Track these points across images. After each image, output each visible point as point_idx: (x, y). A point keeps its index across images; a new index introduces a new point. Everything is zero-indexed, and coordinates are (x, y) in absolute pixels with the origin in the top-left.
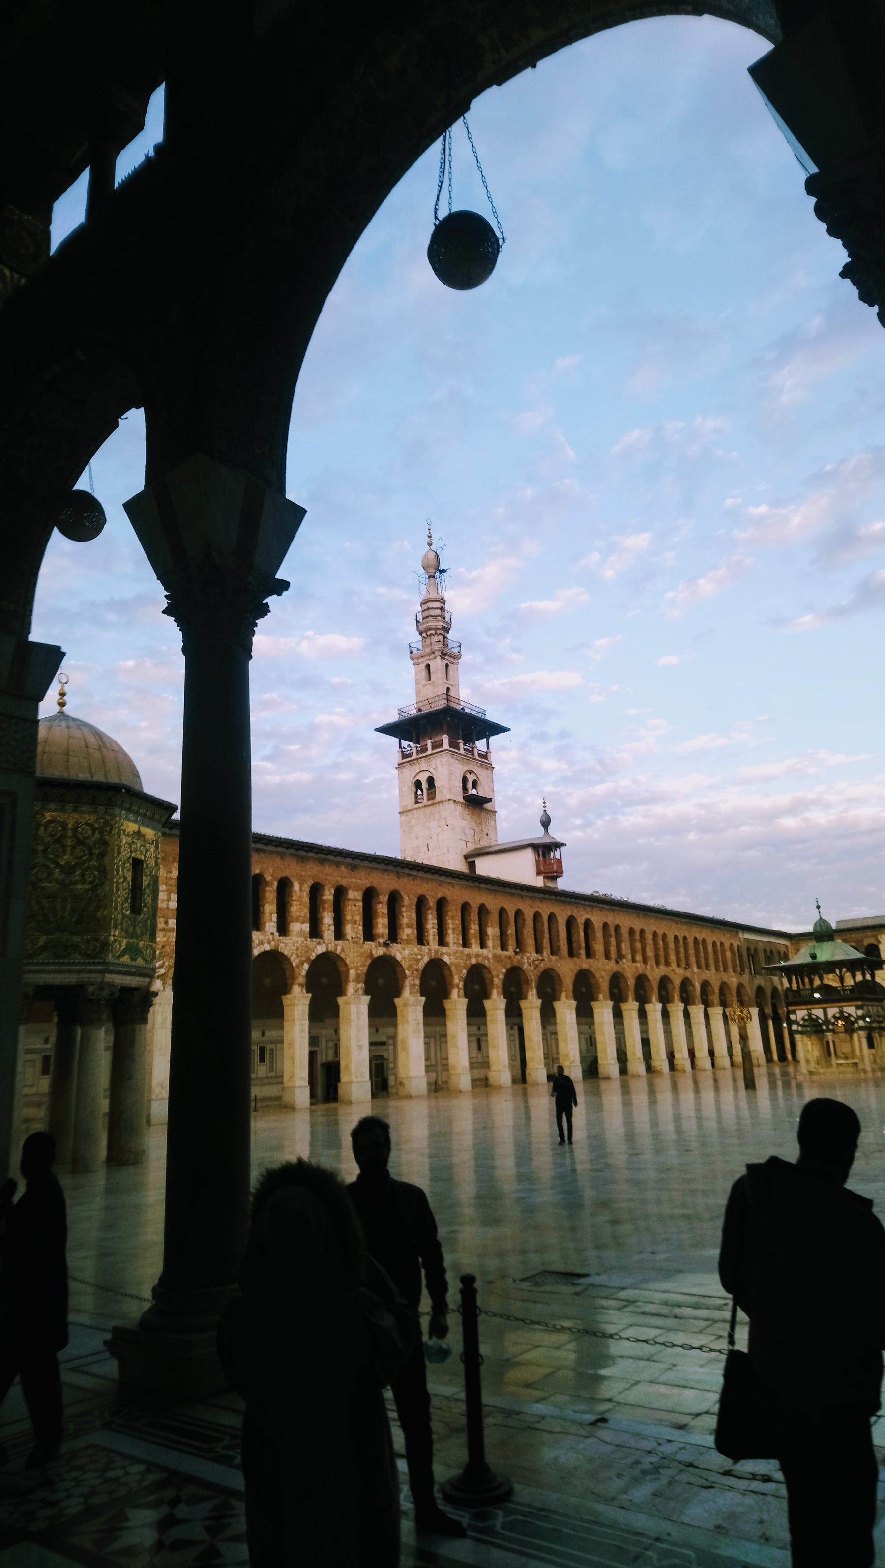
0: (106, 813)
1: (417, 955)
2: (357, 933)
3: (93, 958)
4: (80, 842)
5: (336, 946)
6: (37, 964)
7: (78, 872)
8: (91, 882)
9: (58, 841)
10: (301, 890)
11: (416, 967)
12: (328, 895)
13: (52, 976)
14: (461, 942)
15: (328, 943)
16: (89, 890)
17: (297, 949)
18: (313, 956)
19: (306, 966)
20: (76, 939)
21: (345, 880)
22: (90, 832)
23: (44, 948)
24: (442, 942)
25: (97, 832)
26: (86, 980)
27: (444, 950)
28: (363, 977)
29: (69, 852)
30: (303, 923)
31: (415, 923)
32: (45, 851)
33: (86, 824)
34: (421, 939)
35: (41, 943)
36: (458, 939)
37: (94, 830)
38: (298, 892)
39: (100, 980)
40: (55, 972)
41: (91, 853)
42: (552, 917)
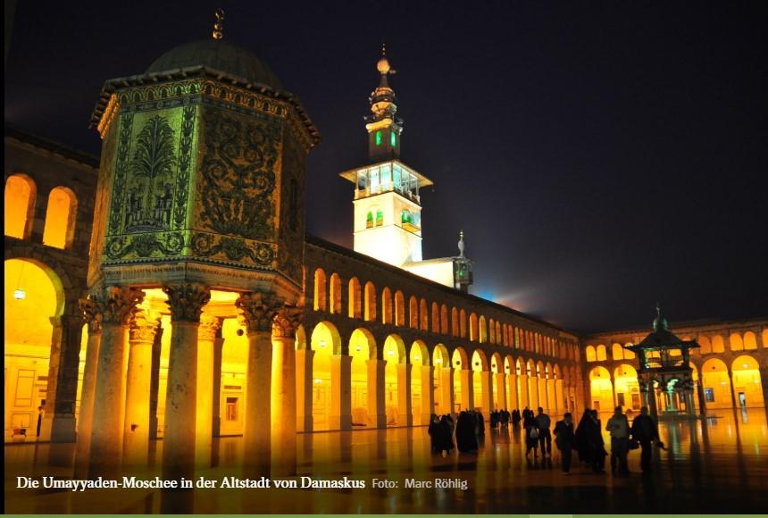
6: (213, 263)
7: (251, 175)
9: (232, 141)
16: (260, 195)
20: (248, 242)
22: (261, 138)
23: (219, 248)
25: (267, 140)
32: (221, 148)
37: (264, 137)
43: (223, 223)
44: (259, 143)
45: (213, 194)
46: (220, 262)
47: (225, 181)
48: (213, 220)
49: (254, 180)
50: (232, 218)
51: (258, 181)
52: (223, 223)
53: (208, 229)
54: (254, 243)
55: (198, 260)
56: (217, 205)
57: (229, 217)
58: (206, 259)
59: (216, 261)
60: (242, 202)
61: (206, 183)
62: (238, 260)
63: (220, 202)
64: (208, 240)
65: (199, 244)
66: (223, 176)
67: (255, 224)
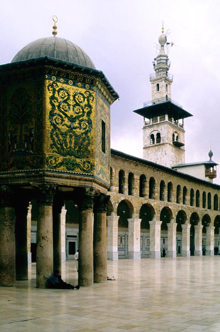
0: (90, 89)
1: (159, 204)
2: (137, 193)
3: (87, 172)
4: (77, 104)
5: (129, 197)
7: (77, 122)
8: (84, 129)
9: (65, 101)
10: (115, 172)
11: (158, 209)
12: (126, 176)
13: (66, 180)
14: (176, 201)
15: (125, 196)
16: (84, 133)
17: (114, 197)
18: (120, 201)
19: (117, 205)
20: (78, 160)
21: (133, 170)
22: (82, 99)
23: (61, 164)
24: (169, 200)
25: (86, 99)
26: (83, 185)
27: (170, 203)
28: (139, 212)
29: (72, 109)
30: (116, 186)
31: (159, 191)
32: (59, 107)
33: (80, 93)
34: (161, 198)
35: (60, 161)
36: (175, 200)
37: (84, 98)
38: (114, 173)
39: (91, 185)
40: (67, 178)
41: (83, 112)
42: (209, 195)
43: (63, 150)
44: (81, 102)
45: (57, 133)
46: (63, 171)
47: (63, 126)
48: (58, 148)
49: (80, 124)
50: (68, 147)
51: (82, 125)
52: (63, 150)
53: (55, 154)
54: (81, 161)
55: (50, 171)
56: (59, 140)
57: (66, 146)
58: (55, 170)
59: (60, 171)
60: (73, 137)
61: (52, 127)
62: (73, 170)
63: (61, 138)
64: (55, 159)
65: (50, 162)
66: (62, 123)
67: (82, 150)
